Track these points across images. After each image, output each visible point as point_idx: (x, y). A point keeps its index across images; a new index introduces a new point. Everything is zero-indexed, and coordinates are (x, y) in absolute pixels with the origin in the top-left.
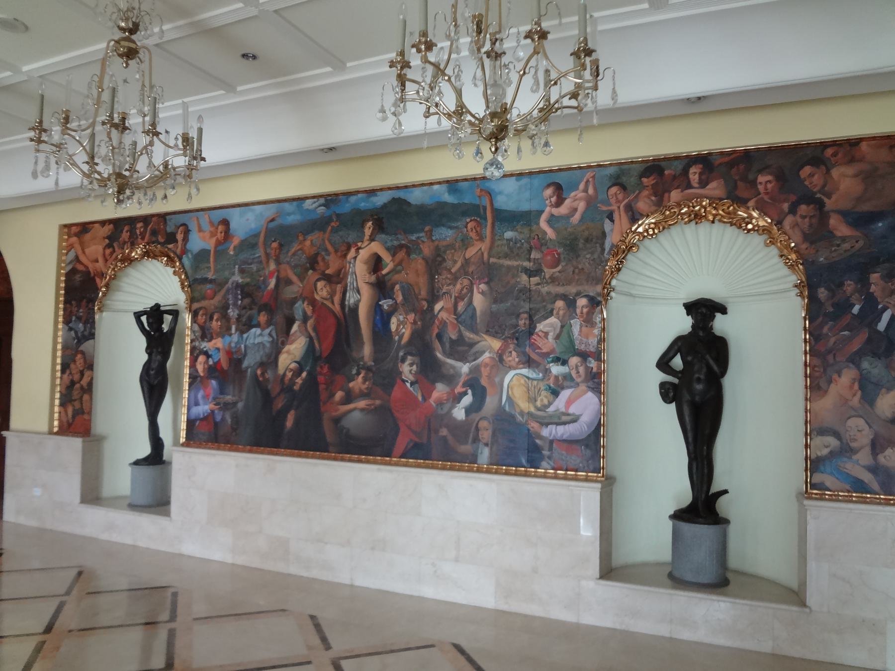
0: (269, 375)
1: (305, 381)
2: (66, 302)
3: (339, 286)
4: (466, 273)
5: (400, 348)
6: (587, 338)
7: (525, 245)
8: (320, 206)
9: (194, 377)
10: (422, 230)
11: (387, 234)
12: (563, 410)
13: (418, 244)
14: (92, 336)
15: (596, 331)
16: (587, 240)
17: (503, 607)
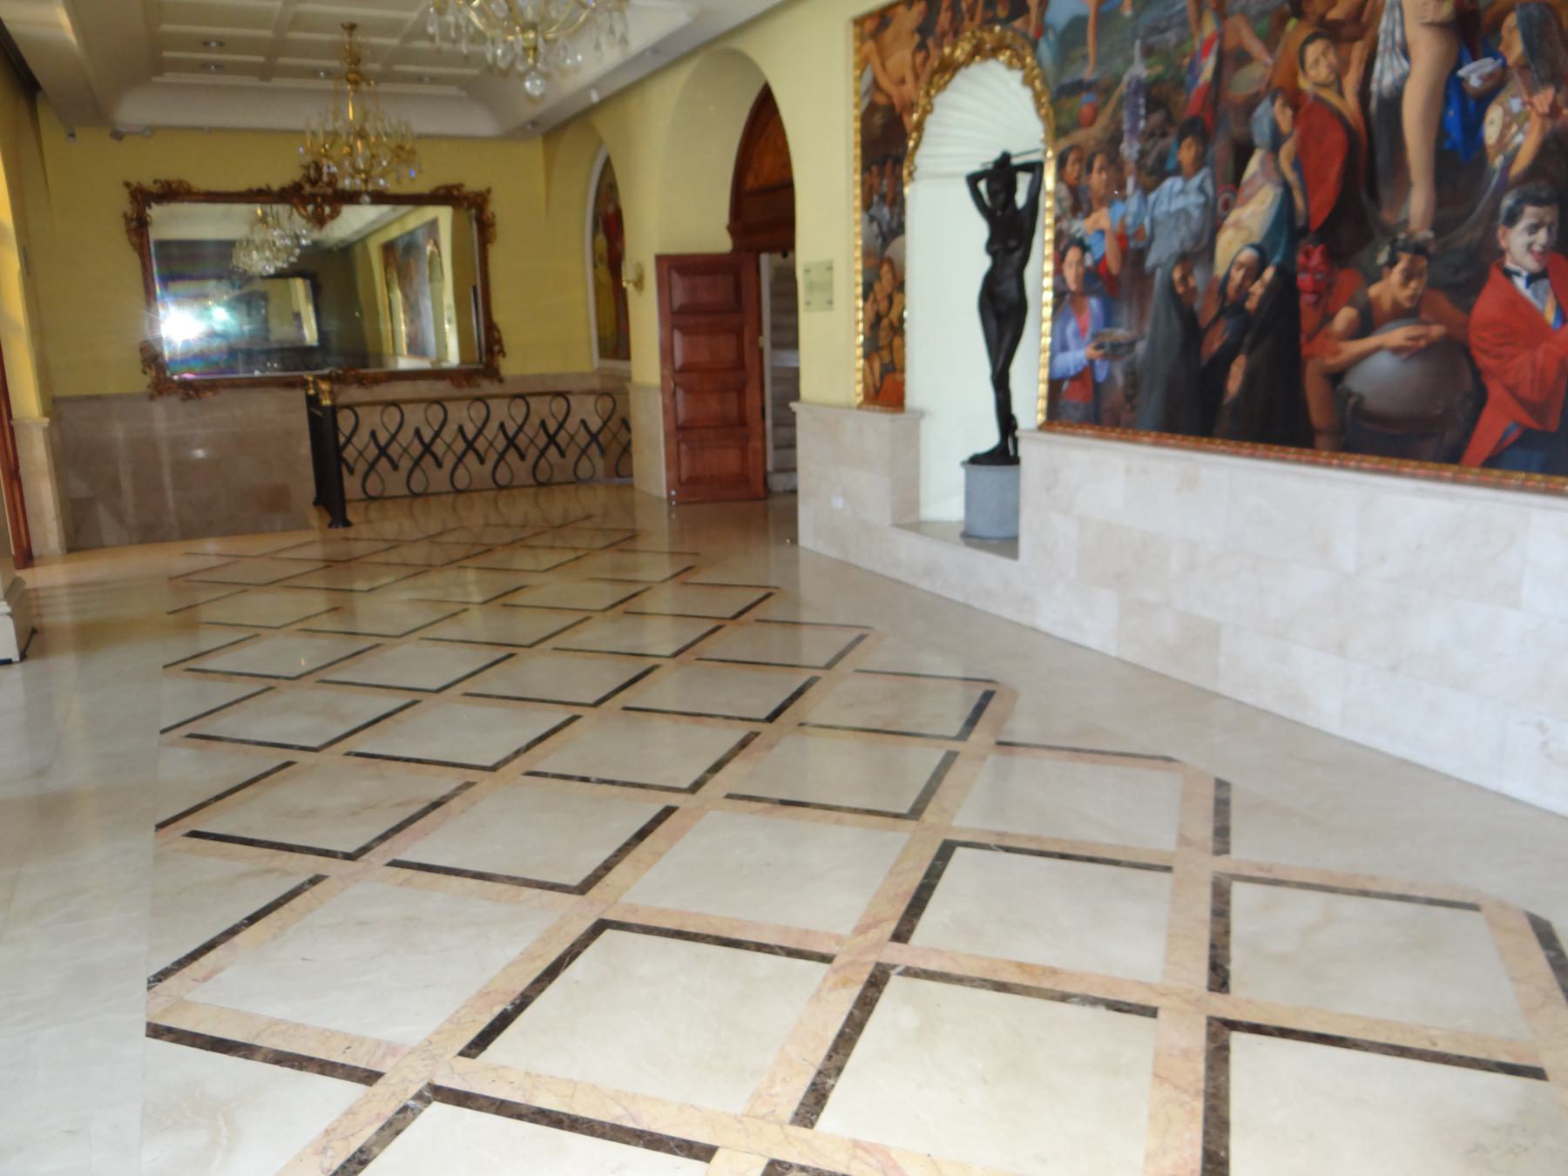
0: (1198, 279)
1: (1270, 288)
2: (866, 168)
5: (1504, 187)
9: (1060, 294)
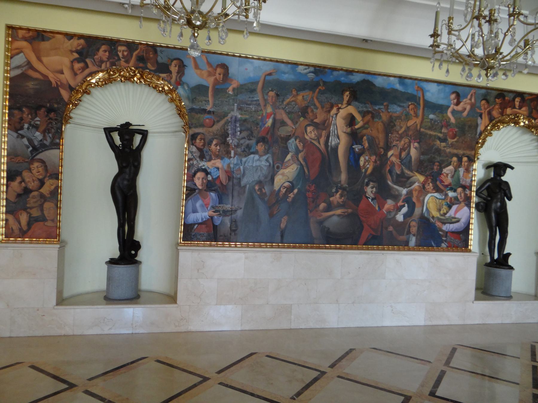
0: (267, 189)
3: (324, 131)
4: (407, 135)
5: (365, 176)
6: (466, 178)
7: (440, 124)
8: (310, 72)
10: (382, 104)
11: (359, 102)
12: (453, 216)
13: (379, 113)
14: (56, 145)
15: (470, 175)
16: (470, 127)
17: (429, 323)
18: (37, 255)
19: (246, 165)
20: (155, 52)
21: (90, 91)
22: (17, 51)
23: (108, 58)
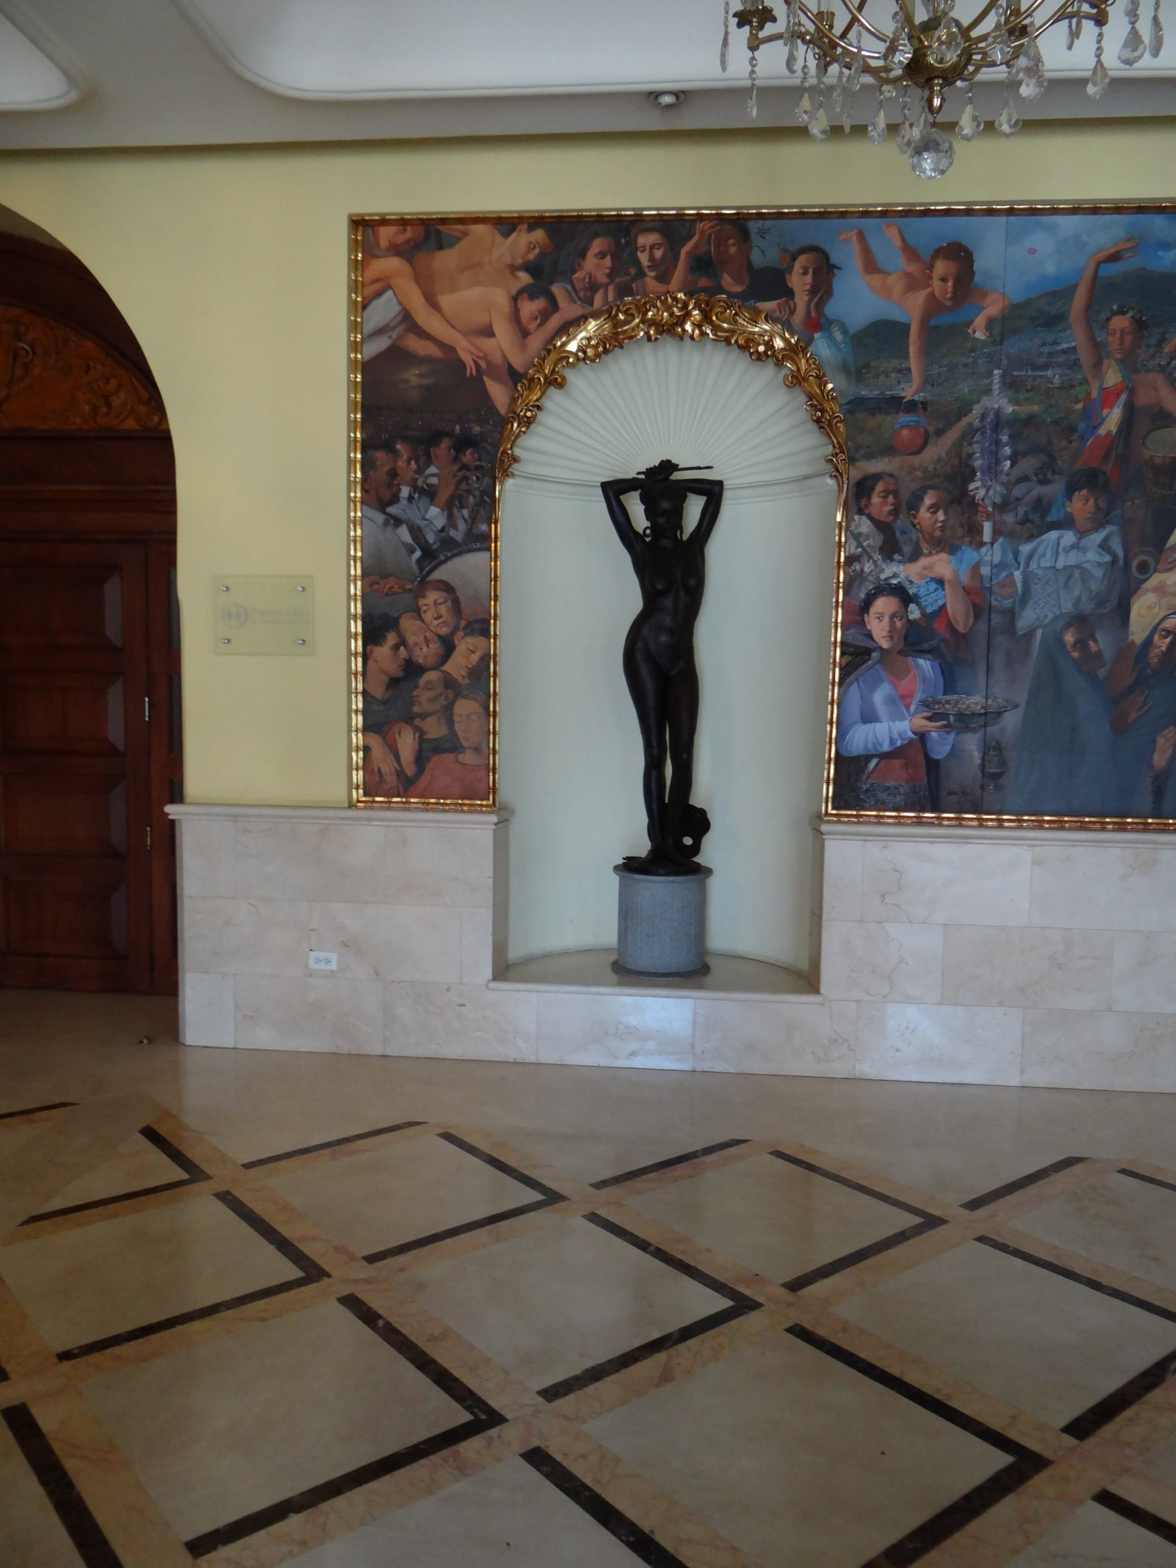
0: (1103, 643)
14: (482, 541)
18: (441, 842)
19: (1033, 565)
20: (745, 235)
21: (564, 379)
22: (377, 286)
23: (609, 276)
